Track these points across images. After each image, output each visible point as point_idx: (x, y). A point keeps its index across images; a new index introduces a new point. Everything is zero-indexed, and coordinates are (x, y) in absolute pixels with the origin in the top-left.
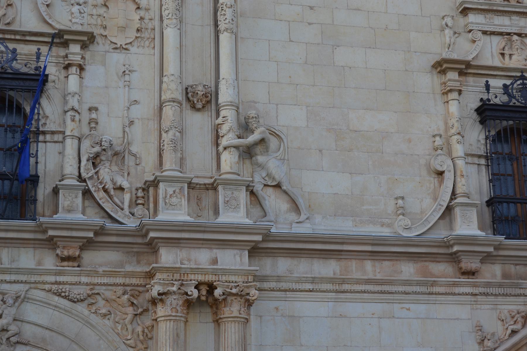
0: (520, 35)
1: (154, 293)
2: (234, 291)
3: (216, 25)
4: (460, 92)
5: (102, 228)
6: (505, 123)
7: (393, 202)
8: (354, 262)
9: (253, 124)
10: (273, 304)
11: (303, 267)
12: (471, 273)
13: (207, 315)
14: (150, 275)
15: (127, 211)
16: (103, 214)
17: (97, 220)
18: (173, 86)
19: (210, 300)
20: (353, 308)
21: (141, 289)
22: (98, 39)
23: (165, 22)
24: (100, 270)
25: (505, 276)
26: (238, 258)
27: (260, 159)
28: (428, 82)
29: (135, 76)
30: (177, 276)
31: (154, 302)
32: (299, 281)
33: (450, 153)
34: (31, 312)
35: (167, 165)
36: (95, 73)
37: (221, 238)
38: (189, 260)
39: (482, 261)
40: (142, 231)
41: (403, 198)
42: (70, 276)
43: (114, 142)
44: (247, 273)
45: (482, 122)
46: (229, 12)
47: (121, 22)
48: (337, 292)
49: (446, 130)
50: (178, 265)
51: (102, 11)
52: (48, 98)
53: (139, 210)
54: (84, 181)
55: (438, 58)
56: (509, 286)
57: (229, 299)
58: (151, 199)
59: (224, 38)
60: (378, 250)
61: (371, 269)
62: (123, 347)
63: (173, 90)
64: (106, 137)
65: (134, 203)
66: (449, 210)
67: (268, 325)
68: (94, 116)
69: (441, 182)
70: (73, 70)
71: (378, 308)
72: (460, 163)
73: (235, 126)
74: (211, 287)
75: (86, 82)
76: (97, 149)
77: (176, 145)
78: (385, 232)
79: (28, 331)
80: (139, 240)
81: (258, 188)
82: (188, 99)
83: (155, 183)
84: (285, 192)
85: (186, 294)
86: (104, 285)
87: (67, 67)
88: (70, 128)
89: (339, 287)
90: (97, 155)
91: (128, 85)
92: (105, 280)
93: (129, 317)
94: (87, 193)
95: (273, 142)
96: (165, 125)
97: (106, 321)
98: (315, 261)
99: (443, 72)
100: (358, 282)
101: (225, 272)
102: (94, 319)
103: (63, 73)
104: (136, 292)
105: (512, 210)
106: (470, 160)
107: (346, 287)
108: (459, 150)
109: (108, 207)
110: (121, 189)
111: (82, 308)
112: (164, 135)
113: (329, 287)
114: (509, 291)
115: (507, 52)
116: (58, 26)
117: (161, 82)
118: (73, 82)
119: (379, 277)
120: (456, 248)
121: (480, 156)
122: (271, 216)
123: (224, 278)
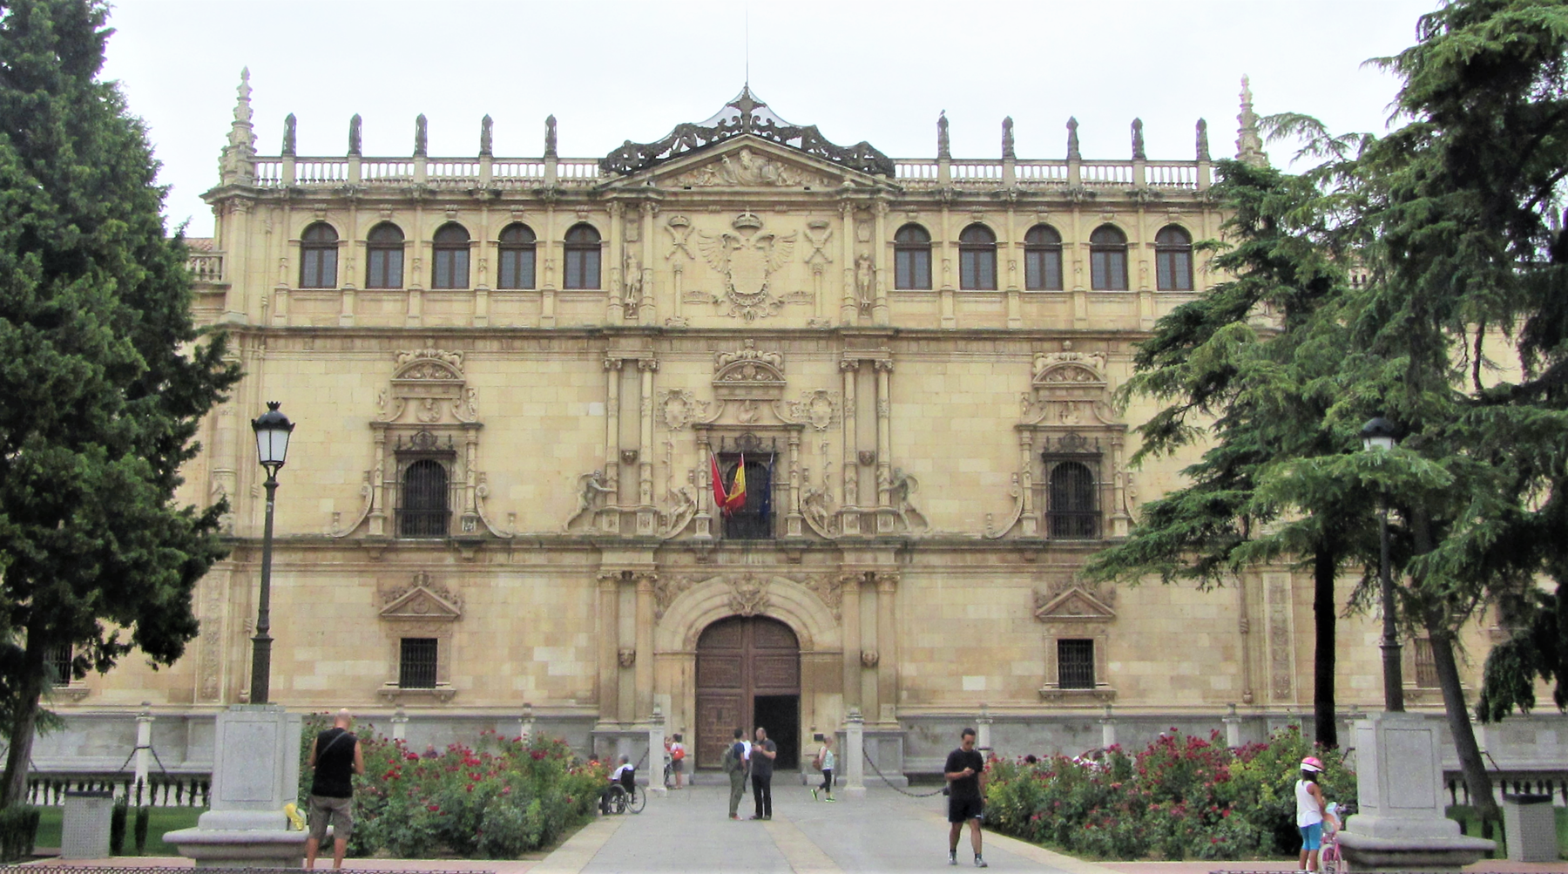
34: (772, 587)
55: (1017, 422)
65: (830, 525)
66: (1019, 521)
74: (873, 575)
79: (774, 599)
81: (902, 512)
83: (839, 514)
88: (795, 483)
94: (803, 520)
95: (909, 482)
109: (815, 527)
111: (802, 586)
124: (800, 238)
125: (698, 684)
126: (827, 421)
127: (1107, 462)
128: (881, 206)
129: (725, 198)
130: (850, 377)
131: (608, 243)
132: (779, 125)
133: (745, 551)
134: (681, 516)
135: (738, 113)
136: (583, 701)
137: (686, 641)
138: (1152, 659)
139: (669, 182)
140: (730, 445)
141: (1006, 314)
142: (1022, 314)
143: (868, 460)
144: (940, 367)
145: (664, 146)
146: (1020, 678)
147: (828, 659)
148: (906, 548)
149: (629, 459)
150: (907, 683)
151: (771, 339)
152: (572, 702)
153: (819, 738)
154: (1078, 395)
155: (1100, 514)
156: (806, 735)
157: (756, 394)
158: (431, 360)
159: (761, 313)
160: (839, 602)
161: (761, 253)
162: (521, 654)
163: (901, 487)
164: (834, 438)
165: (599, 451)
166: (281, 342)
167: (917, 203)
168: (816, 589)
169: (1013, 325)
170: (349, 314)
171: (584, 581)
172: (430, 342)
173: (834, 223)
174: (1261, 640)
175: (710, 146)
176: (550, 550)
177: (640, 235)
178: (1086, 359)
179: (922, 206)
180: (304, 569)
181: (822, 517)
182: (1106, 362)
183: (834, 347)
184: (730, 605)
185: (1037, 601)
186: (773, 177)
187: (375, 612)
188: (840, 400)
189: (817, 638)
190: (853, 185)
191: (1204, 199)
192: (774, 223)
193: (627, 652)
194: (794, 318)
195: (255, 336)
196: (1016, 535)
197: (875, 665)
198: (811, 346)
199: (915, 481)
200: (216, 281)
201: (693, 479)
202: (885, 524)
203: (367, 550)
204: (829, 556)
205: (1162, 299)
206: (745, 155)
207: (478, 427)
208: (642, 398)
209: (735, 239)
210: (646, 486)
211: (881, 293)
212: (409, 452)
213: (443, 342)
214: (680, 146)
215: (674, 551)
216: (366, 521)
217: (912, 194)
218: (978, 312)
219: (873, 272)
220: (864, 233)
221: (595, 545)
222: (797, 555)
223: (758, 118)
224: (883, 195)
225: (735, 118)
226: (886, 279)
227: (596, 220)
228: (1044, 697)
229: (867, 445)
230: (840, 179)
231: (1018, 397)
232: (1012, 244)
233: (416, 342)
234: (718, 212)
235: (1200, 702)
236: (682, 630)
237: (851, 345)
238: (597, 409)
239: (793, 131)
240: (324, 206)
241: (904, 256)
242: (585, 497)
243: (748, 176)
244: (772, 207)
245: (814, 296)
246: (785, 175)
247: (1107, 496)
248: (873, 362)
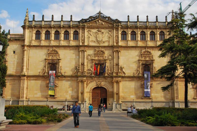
65: (111, 74)
66: (139, 74)
74: (118, 81)
109: (109, 74)
125: (92, 97)
126: (111, 59)
127: (152, 65)
128: (120, 28)
129: (97, 27)
130: (115, 52)
131: (80, 33)
132: (105, 16)
133: (99, 77)
134: (90, 72)
135: (99, 15)
136: (76, 99)
137: (90, 90)
138: (158, 93)
139: (88, 25)
140: (97, 63)
141: (137, 44)
142: (140, 44)
144: (128, 51)
145: (88, 19)
146: (139, 96)
147: (111, 93)
148: (123, 77)
149: (83, 64)
150: (123, 96)
152: (74, 99)
153: (110, 104)
154: (147, 55)
156: (108, 104)
157: (101, 55)
158: (53, 50)
161: (101, 35)
162: (67, 92)
163: (122, 69)
164: (112, 61)
165: (78, 63)
166: (32, 47)
167: (124, 28)
168: (109, 83)
169: (138, 45)
170: (43, 43)
171: (76, 82)
172: (54, 48)
173: (112, 31)
174: (174, 91)
175: (94, 19)
176: (71, 77)
177: (84, 33)
178: (149, 50)
179: (125, 28)
180: (36, 80)
181: (110, 73)
184: (97, 85)
185: (141, 85)
186: (104, 24)
187: (45, 86)
188: (113, 56)
189: (109, 90)
190: (115, 25)
191: (166, 27)
192: (103, 30)
193: (82, 92)
194: (106, 44)
195: (29, 47)
196: (138, 76)
198: (109, 48)
199: (124, 68)
200: (23, 39)
201: (92, 67)
202: (119, 74)
203: (45, 77)
204: (111, 78)
205: (160, 42)
206: (100, 21)
207: (60, 59)
208: (84, 56)
209: (98, 33)
210: (85, 68)
211: (119, 41)
212: (51, 63)
213: (56, 48)
214: (90, 19)
215: (89, 78)
216: (44, 73)
217: (124, 26)
219: (118, 38)
221: (77, 77)
222: (107, 78)
223: (101, 15)
224: (120, 26)
225: (98, 15)
226: (120, 39)
227: (78, 30)
228: (142, 99)
230: (113, 24)
231: (139, 56)
233: (52, 47)
234: (95, 29)
235: (164, 100)
236: (90, 88)
238: (78, 57)
239: (106, 17)
240: (38, 28)
242: (76, 70)
243: (100, 24)
244: (103, 28)
245: (109, 41)
246: (105, 24)
248: (118, 51)
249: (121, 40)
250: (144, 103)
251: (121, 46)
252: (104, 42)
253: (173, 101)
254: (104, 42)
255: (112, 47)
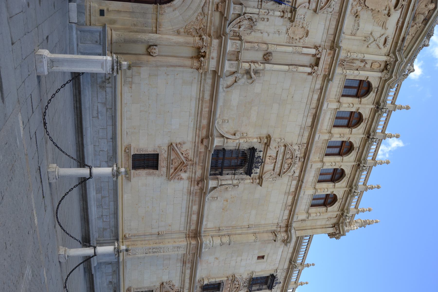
0: (276, 162)
1: (204, 37)
2: (202, 64)
3: (291, 65)
4: (260, 143)
5: (227, 20)
6: (249, 156)
7: (227, 119)
8: (208, 105)
9: (257, 75)
10: (196, 77)
11: (208, 88)
12: (202, 142)
13: (194, 54)
14: (210, 36)
15: (232, 29)
16: (232, 20)
17: (230, 19)
18: (273, 48)
19: (200, 56)
20: (193, 104)
21: (205, 32)
22: (291, 24)
23: (294, 48)
24: (213, 18)
25: (200, 152)
26: (213, 66)
27: (245, 76)
28: (264, 133)
29: (277, 35)
30: (209, 45)
31: (200, 36)
32: (204, 86)
33: (241, 138)
35: (246, 44)
36: (279, 22)
37: (220, 61)
38: (214, 50)
39: (206, 146)
40: (225, 34)
41: (228, 122)
42: (212, 7)
43: (256, 26)
44: (208, 69)
45: (250, 149)
46: (295, 70)
47: (296, 32)
48: (199, 99)
49: (248, 137)
50: (212, 46)
51: (301, 26)
52: (273, 4)
53: (232, 33)
54: (244, 15)
55: (271, 136)
56: (197, 153)
57: (200, 63)
58: (235, 38)
59: (286, 67)
60: (212, 113)
61: (206, 110)
62: (186, 24)
63: (272, 48)
64: (258, 24)
65: (234, 32)
66: (223, 136)
67: (190, 75)
68: (266, 20)
69: (232, 135)
70: (282, 14)
71: (193, 111)
72: (237, 141)
73: (257, 69)
74: (204, 57)
75: (277, 18)
76: (254, 20)
77: (253, 48)
78: (218, 116)
80: (222, 33)
81: (236, 75)
82: (268, 53)
83: (240, 40)
84: (233, 84)
85: (202, 48)
86: (207, 19)
87: (283, 12)
88: (262, 11)
89: (201, 100)
90: (252, 20)
91: (275, 33)
92: (209, 19)
93: (196, 27)
94: (239, 15)
95: (250, 81)
96: (260, 44)
97: (195, 19)
98: (210, 92)
99: (267, 138)
100: (202, 106)
101: (209, 62)
102: (196, 15)
103: (281, 10)
104: (204, 30)
105: (221, 156)
106: (238, 144)
107: (201, 102)
108: (242, 141)
109: (234, 22)
110: (240, 28)
112: (257, 44)
113: (201, 96)
114: (195, 153)
115: (271, 158)
116: (297, 10)
117: (274, 44)
118: (278, 14)
119: (203, 112)
120: (210, 138)
121: (239, 147)
122: (226, 78)
123: (207, 61)
124: (383, 31)
130: (313, 51)
143: (267, 58)
151: (341, 8)
155: (221, 174)
159: (355, 3)
160: (188, 33)
161: (384, 8)
173: (385, 50)
182: (289, 176)
183: (328, 44)
186: (417, 20)
196: (215, 133)
197: (149, 54)
198: (332, 31)
218: (326, 120)
220: (376, 66)
229: (275, 58)
232: (351, 136)
237: (330, 54)
241: (356, 85)
245: (354, 35)
247: (229, 177)
248: (317, 64)
249: (347, 78)
250: (111, 154)
251: (332, 80)
252: (357, 16)
253: (120, 240)
254: (357, 16)
255: (334, 46)
